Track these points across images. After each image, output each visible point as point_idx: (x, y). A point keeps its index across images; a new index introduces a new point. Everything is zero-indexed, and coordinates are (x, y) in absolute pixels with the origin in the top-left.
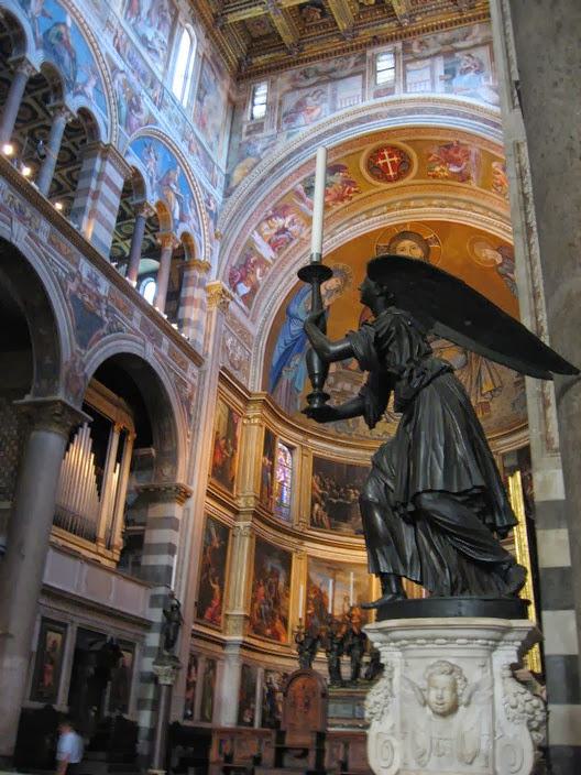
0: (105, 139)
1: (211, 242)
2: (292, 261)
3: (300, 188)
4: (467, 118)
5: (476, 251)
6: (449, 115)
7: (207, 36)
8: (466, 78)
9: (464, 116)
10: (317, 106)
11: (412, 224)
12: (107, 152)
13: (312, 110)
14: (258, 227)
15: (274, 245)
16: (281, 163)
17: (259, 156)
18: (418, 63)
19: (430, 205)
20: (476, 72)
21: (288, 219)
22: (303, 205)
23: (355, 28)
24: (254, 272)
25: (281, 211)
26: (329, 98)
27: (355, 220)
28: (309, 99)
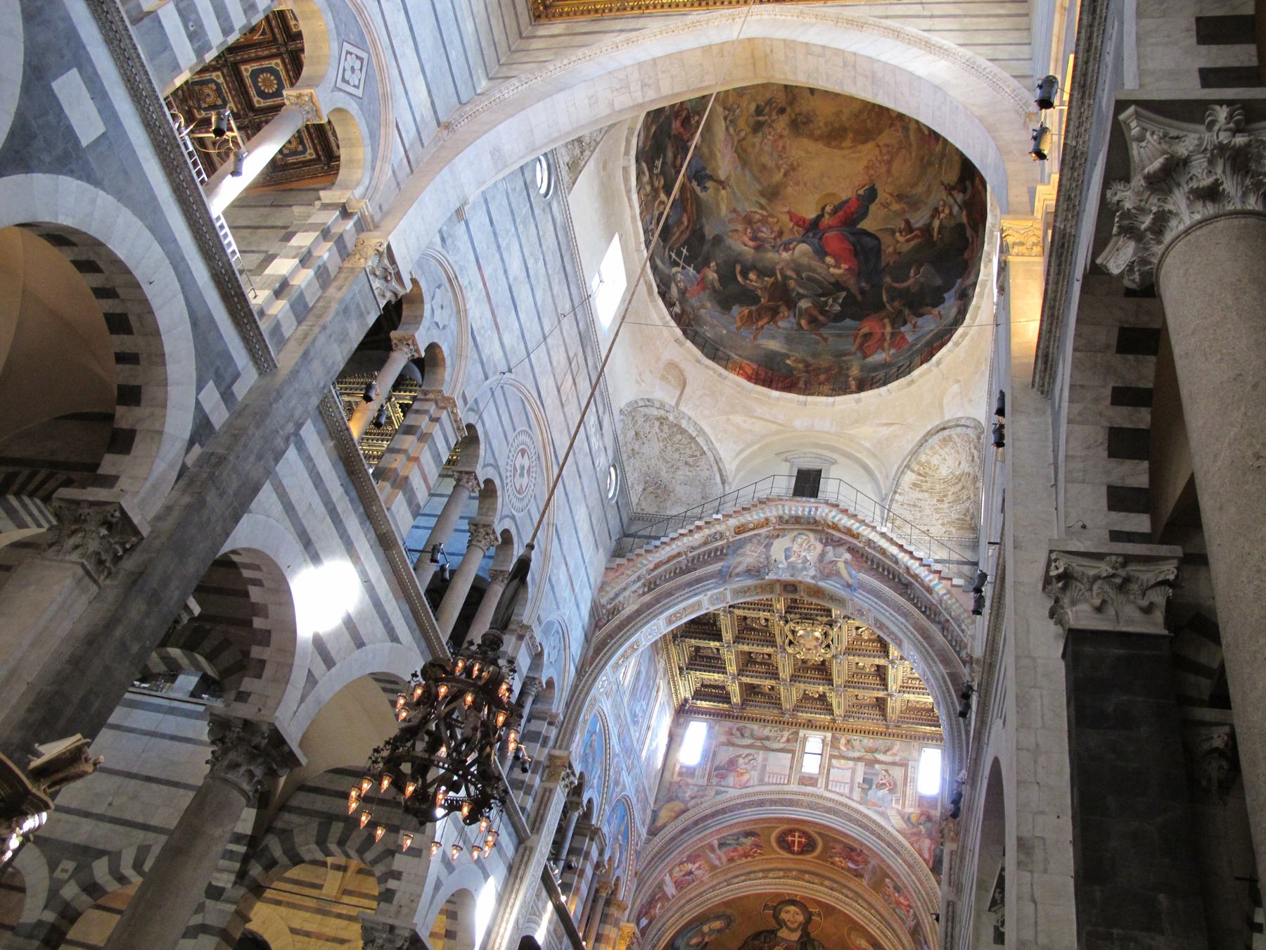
0: (594, 822)
1: (631, 880)
2: (687, 899)
3: (716, 843)
4: (874, 834)
5: (852, 937)
6: (860, 826)
7: (669, 683)
8: (881, 793)
9: (873, 832)
10: (747, 771)
11: (802, 897)
12: (595, 833)
13: (742, 774)
14: (671, 872)
15: (679, 885)
16: (705, 818)
17: (685, 802)
18: (843, 762)
19: (822, 884)
20: (889, 790)
21: (697, 865)
22: (712, 855)
23: (797, 708)
24: (655, 907)
25: (692, 858)
26: (759, 767)
27: (752, 876)
28: (741, 761)
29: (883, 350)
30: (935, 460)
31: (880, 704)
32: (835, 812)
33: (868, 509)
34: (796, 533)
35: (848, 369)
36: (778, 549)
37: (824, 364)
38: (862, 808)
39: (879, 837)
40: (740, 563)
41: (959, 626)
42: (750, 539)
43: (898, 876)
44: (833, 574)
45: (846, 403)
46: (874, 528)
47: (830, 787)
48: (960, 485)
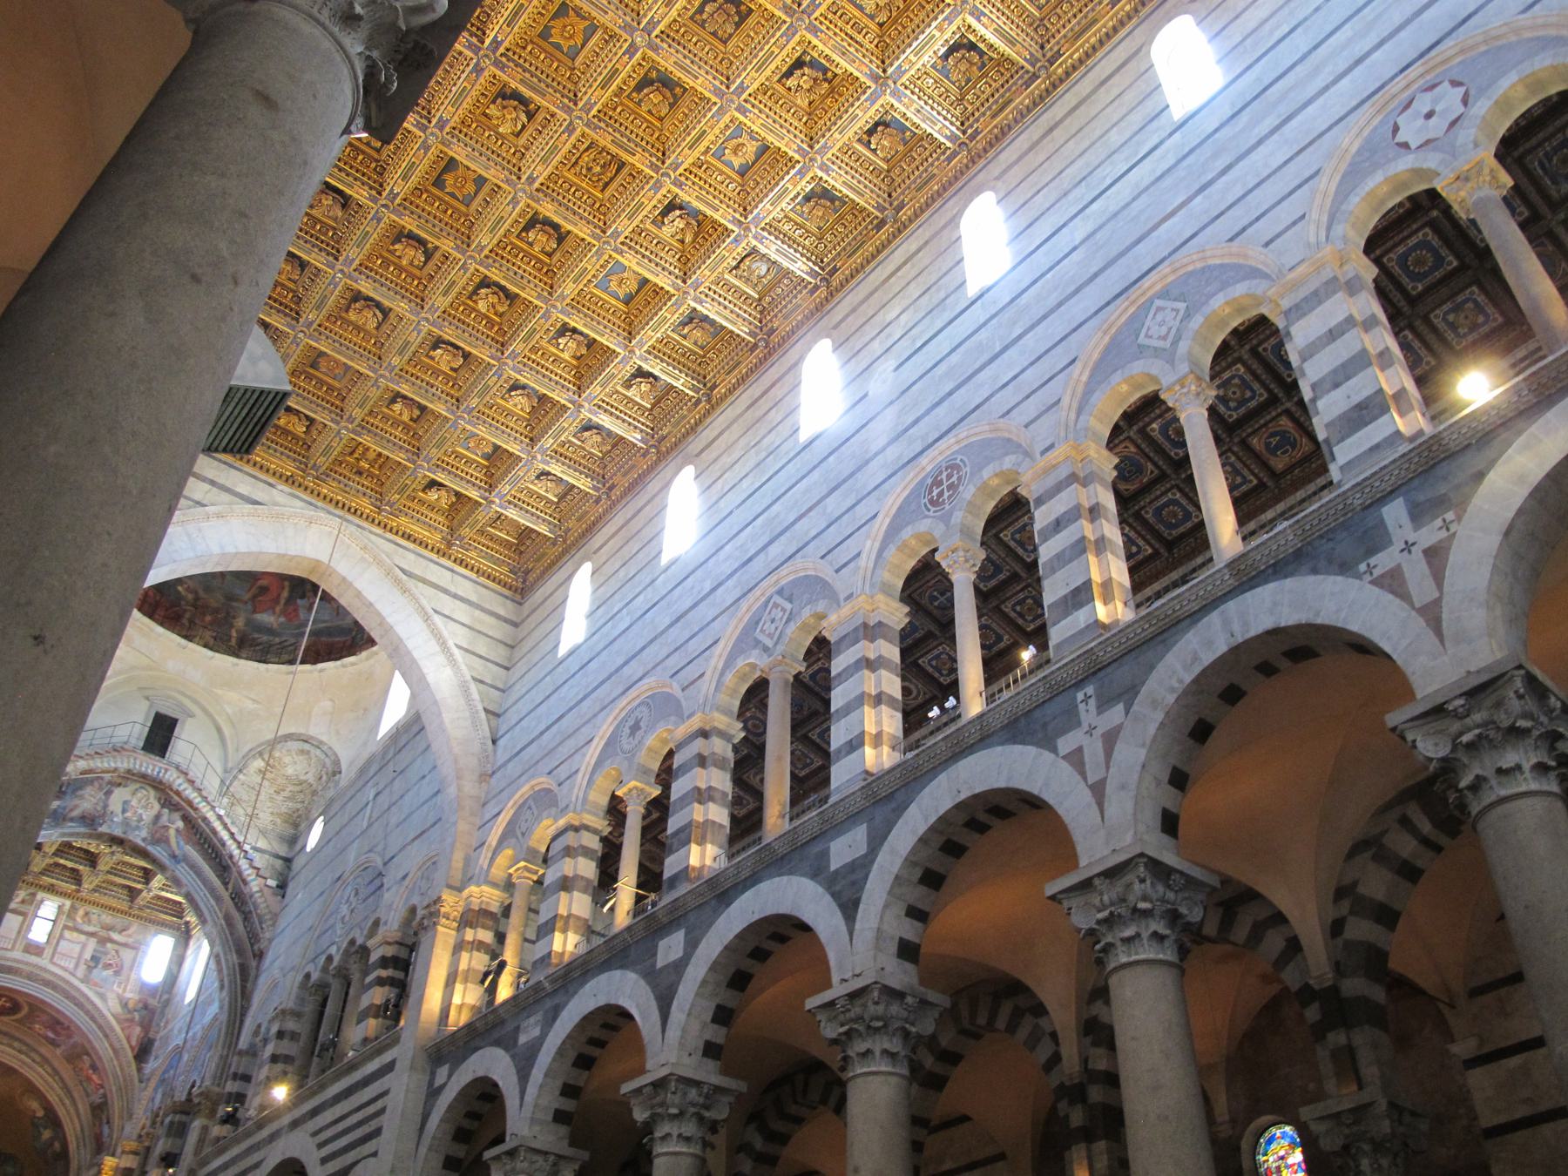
6: (76, 1004)
9: (87, 1012)
18: (75, 934)
23: (44, 872)
29: (274, 613)
30: (287, 760)
31: (133, 893)
32: (55, 987)
33: (212, 784)
34: (138, 785)
35: (234, 618)
36: (119, 795)
37: (214, 604)
38: (83, 987)
39: (93, 1018)
40: (76, 806)
41: (261, 923)
42: (91, 782)
43: (100, 1058)
44: (161, 840)
45: (224, 662)
46: (213, 808)
47: (55, 960)
48: (299, 788)
